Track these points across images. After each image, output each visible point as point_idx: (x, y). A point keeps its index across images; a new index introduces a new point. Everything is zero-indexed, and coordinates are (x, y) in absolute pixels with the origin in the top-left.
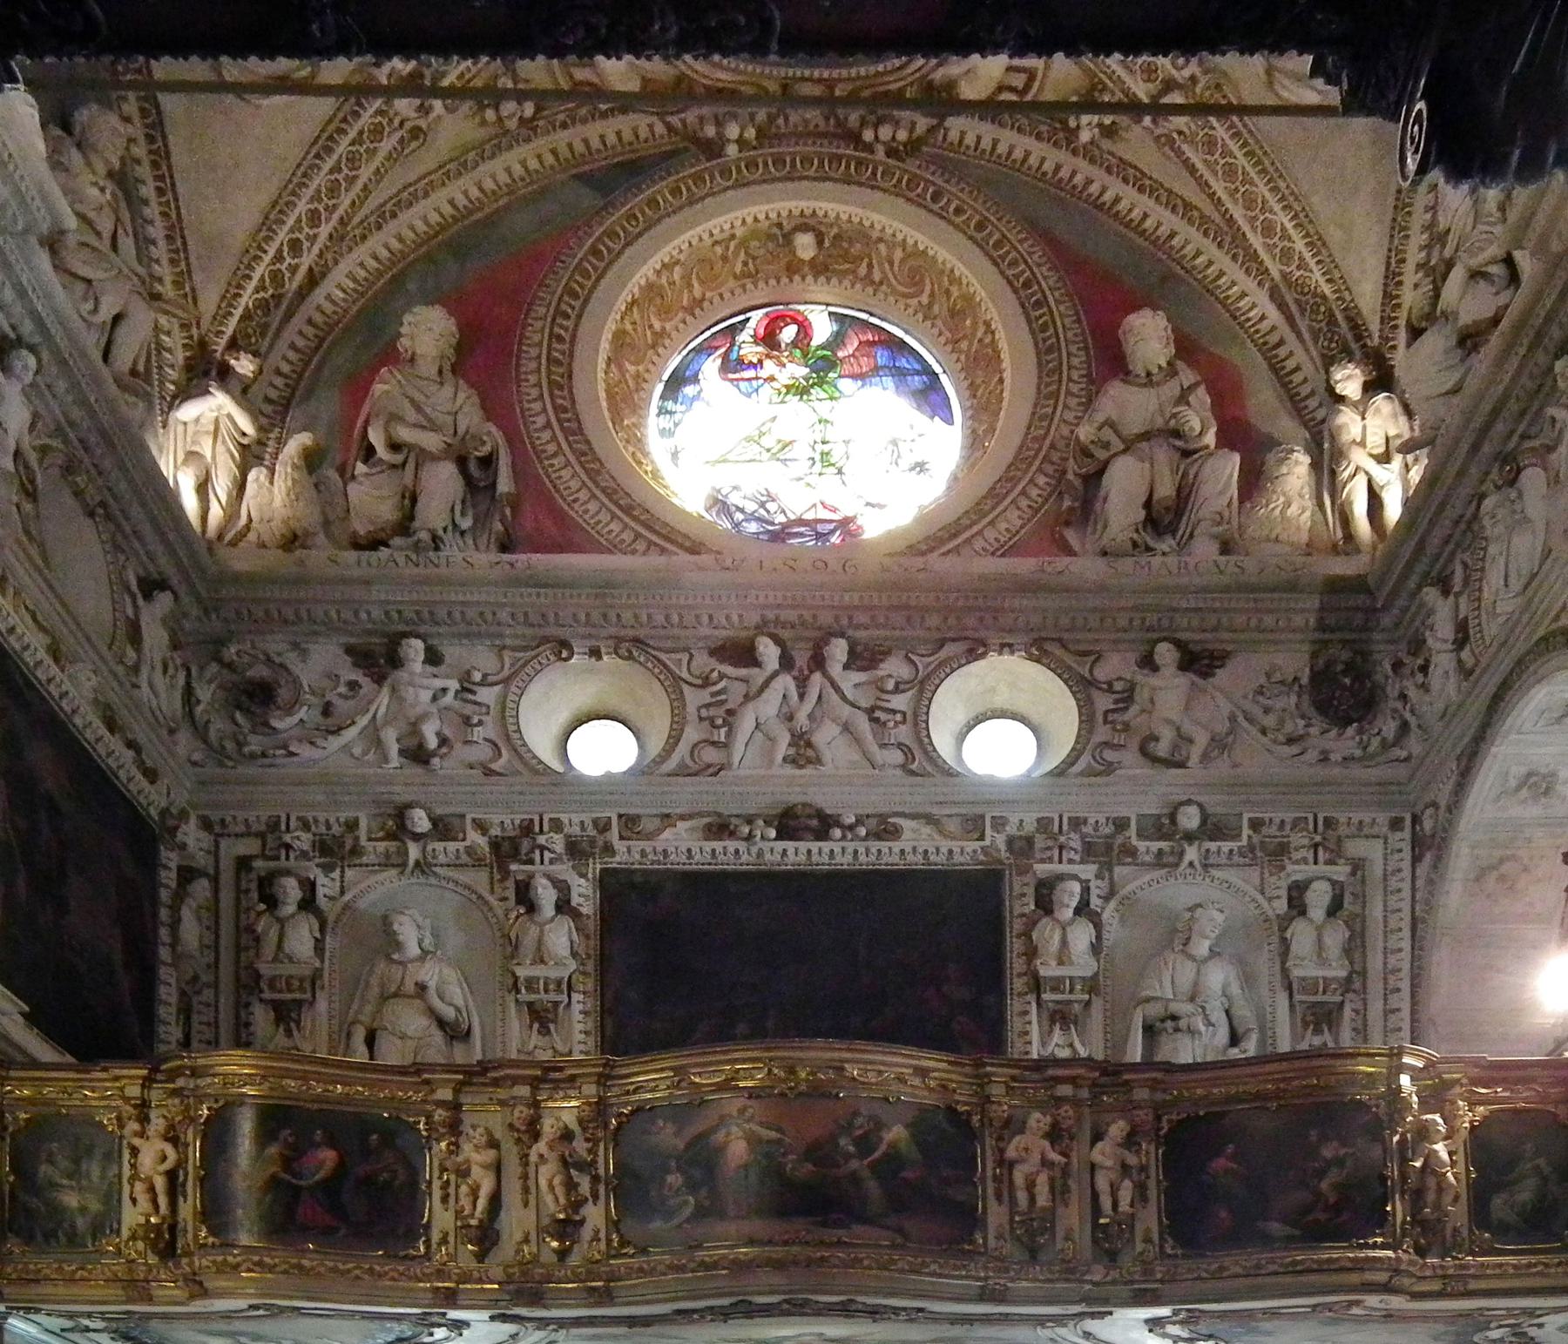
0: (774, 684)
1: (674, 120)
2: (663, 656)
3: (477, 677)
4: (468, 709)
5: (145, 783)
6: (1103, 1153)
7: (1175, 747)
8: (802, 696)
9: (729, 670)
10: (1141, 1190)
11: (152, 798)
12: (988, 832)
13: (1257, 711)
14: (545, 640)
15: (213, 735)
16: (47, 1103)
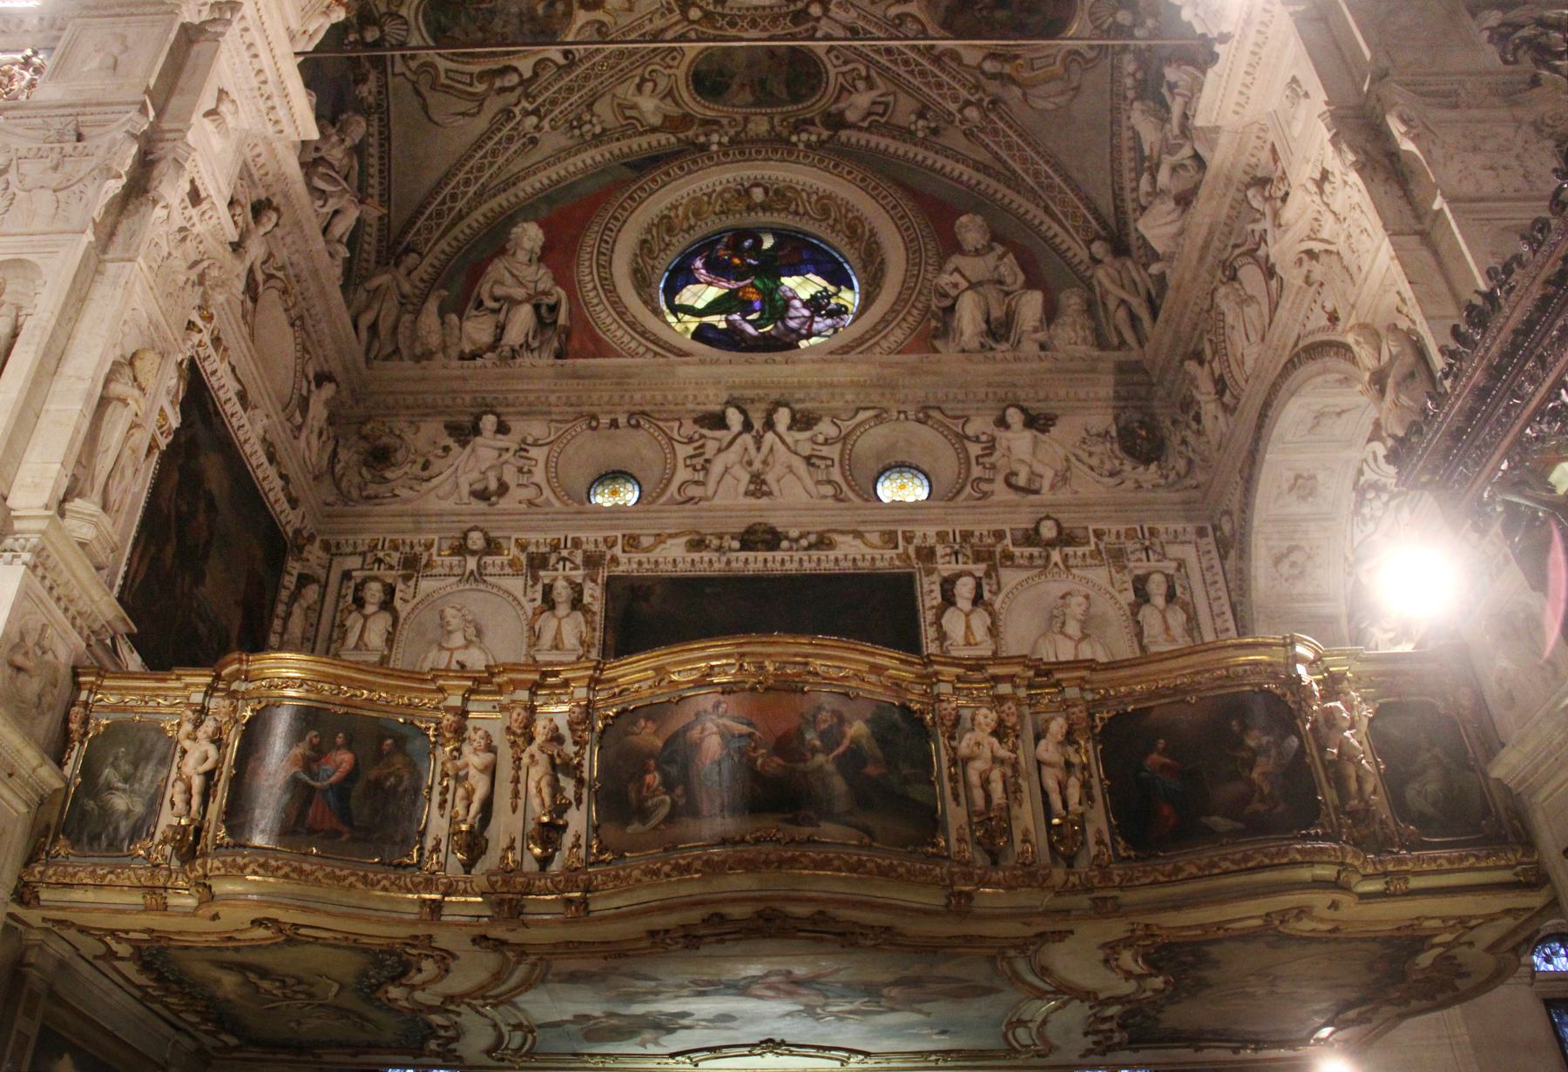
0: (739, 441)
1: (681, 136)
2: (661, 424)
3: (530, 440)
4: (521, 462)
5: (286, 506)
6: (1048, 750)
7: (1030, 480)
8: (758, 449)
9: (705, 432)
10: (1086, 786)
11: (290, 519)
12: (901, 542)
13: (1084, 456)
14: (581, 415)
15: (344, 484)
16: (125, 709)
